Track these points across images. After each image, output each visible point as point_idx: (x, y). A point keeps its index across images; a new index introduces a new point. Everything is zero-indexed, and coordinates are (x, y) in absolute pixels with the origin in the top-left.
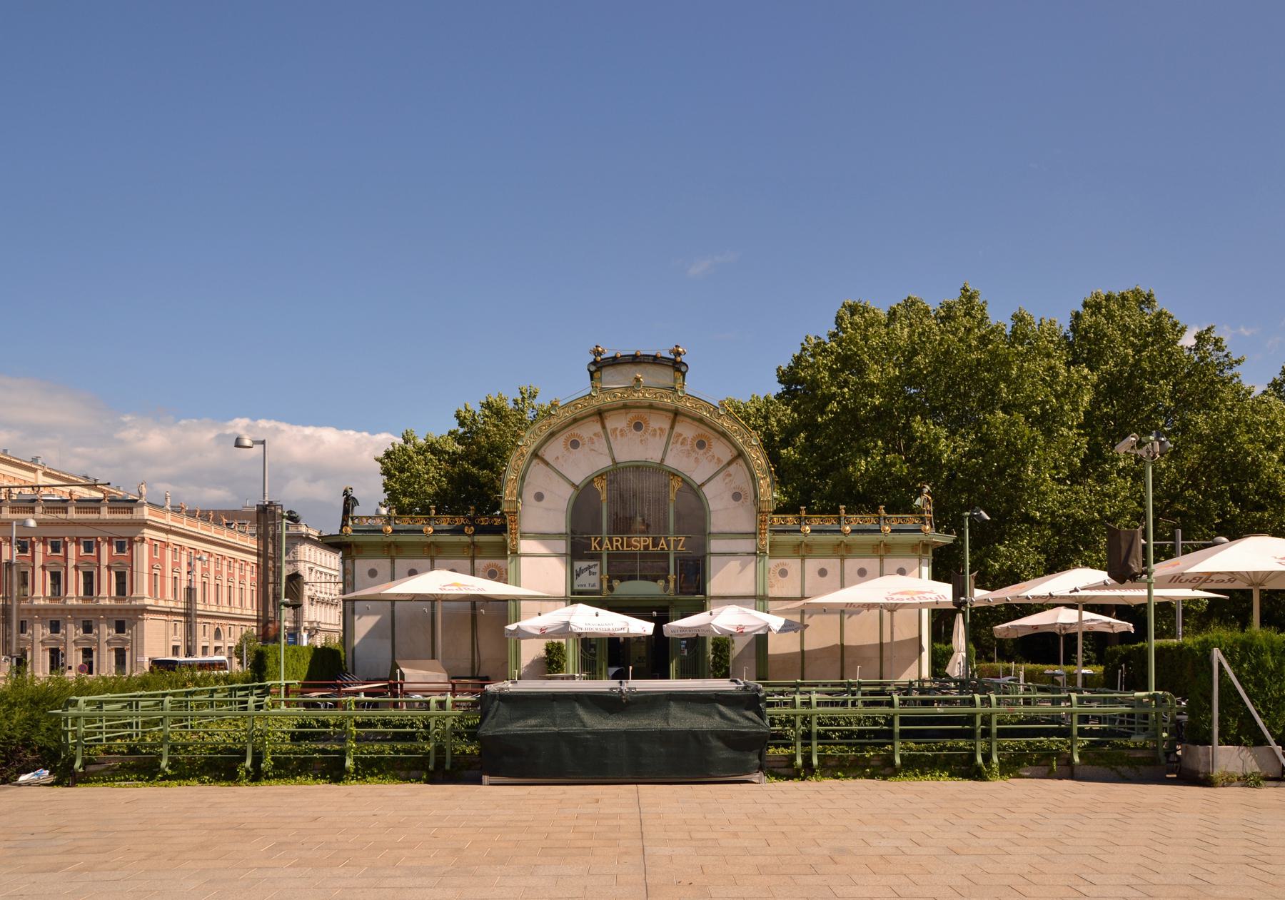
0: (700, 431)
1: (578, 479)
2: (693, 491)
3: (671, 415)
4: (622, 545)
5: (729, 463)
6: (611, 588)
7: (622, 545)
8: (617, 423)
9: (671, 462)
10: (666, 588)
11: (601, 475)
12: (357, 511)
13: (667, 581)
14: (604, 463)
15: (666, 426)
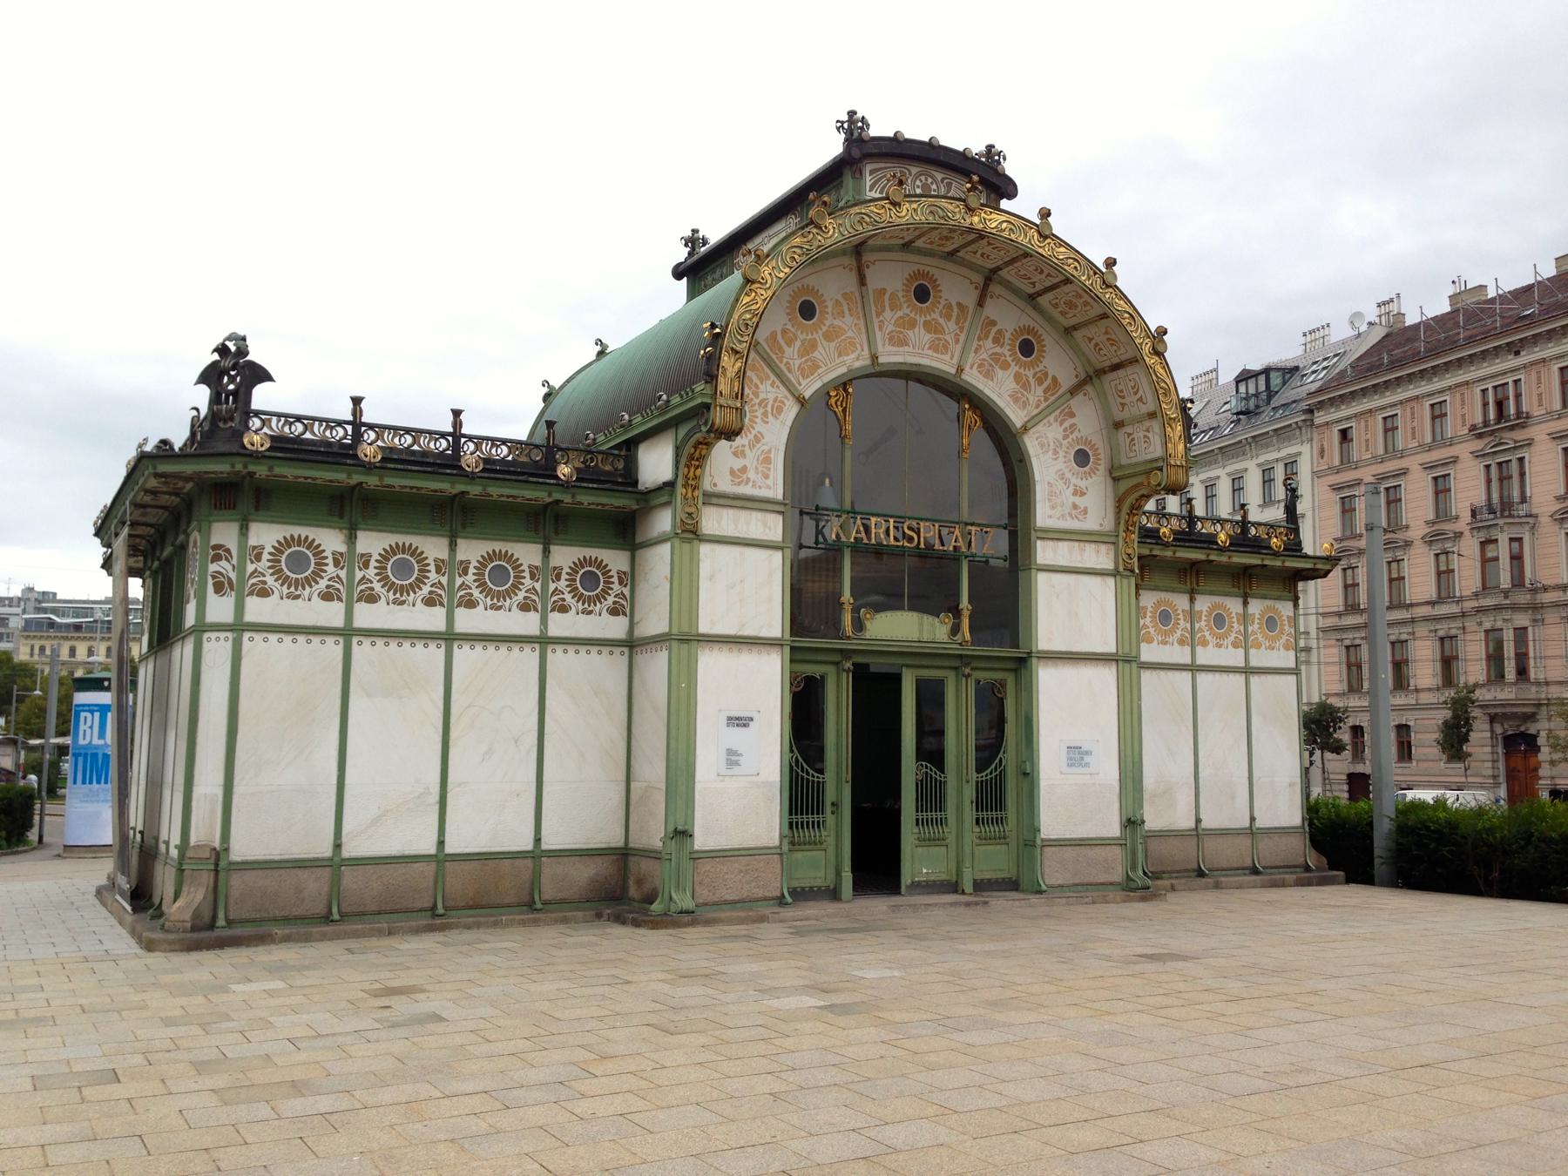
0: (1026, 321)
1: (809, 388)
2: (1005, 444)
3: (979, 279)
4: (887, 532)
5: (1073, 391)
6: (859, 625)
7: (887, 532)
8: (889, 276)
9: (973, 378)
10: (955, 630)
11: (844, 384)
12: (262, 397)
13: (957, 613)
14: (857, 360)
15: (970, 300)
